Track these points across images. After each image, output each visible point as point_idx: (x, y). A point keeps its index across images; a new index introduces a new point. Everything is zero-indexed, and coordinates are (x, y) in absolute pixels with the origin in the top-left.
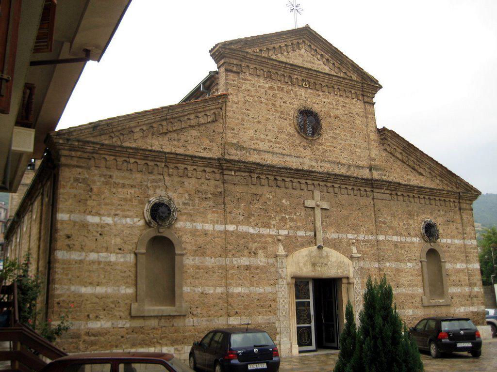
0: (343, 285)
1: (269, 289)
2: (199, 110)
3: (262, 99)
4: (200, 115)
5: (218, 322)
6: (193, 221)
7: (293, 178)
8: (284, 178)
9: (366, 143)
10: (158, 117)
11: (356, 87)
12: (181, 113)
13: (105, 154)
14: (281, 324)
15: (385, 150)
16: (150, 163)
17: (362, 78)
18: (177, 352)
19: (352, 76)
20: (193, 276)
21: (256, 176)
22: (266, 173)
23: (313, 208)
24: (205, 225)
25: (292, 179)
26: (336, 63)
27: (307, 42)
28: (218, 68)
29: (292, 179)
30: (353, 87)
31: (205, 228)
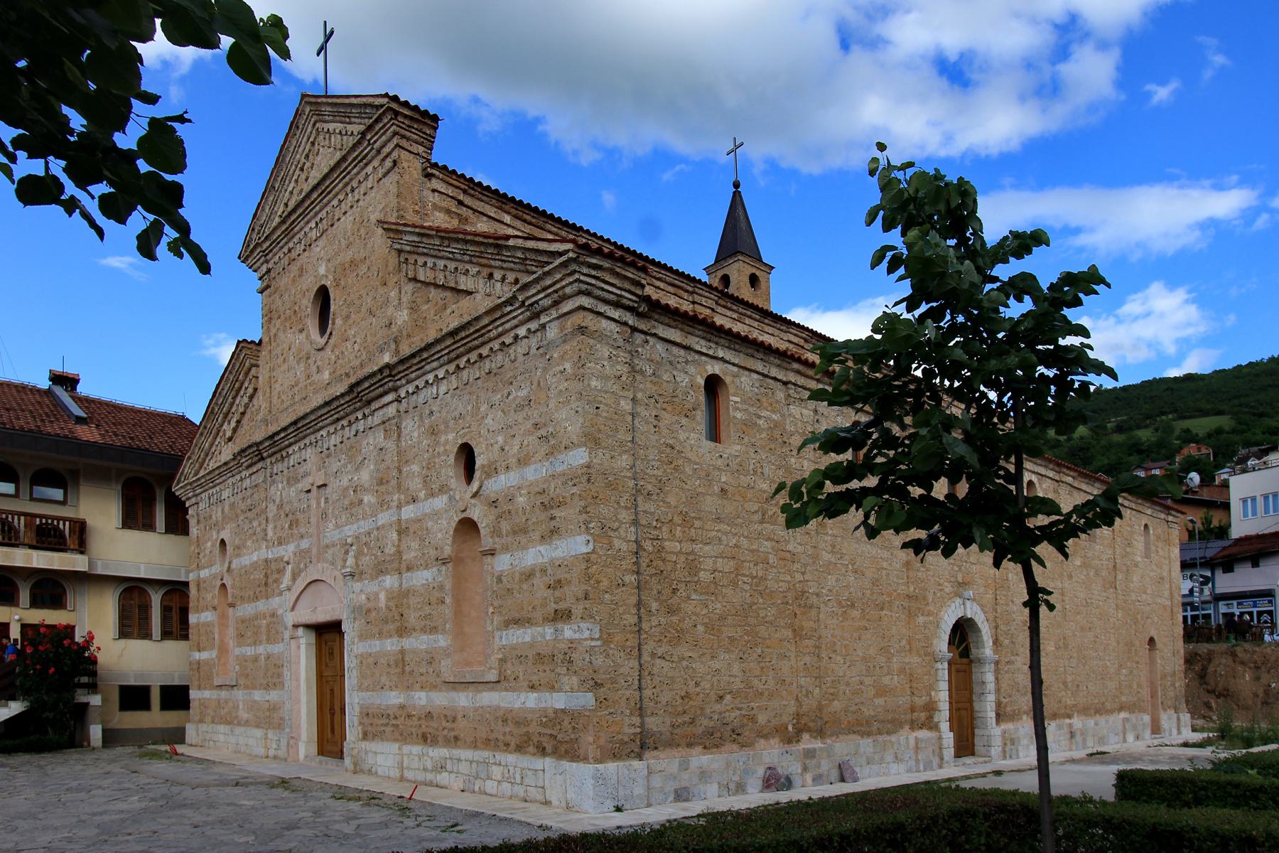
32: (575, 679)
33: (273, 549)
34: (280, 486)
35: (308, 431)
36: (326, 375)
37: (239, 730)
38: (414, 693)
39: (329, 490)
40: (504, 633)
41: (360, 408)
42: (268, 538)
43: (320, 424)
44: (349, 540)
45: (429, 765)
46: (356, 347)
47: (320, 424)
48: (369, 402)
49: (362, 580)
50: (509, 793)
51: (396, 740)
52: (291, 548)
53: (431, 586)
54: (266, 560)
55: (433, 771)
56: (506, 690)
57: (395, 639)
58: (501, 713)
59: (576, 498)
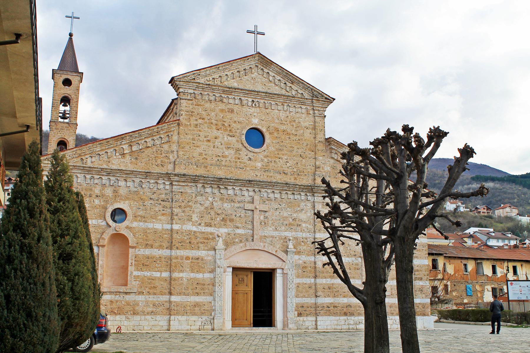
0: (278, 275)
1: (207, 275)
2: (154, 134)
3: (213, 121)
4: (155, 138)
5: (162, 299)
6: (145, 222)
7: (235, 186)
8: (226, 186)
9: (313, 153)
10: (119, 142)
11: (306, 103)
12: (138, 138)
13: (77, 173)
14: (217, 303)
15: (332, 158)
16: (112, 178)
17: (313, 94)
18: (127, 320)
19: (304, 93)
20: (143, 264)
21: (200, 185)
22: (210, 182)
23: (253, 210)
24: (155, 224)
25: (234, 187)
26: (287, 83)
27: (259, 66)
28: (178, 95)
29: (234, 187)
30: (303, 104)
31: (155, 227)
32: (424, 295)
33: (199, 227)
34: (210, 199)
35: (256, 186)
36: (259, 165)
37: (137, 318)
38: (339, 299)
39: (267, 214)
40: (391, 281)
41: (306, 192)
42: (193, 220)
43: (270, 187)
44: (291, 238)
45: (352, 322)
46: (288, 164)
47: (270, 187)
48: (314, 192)
49: (300, 255)
50: (396, 328)
51: (329, 315)
52: (223, 231)
53: (351, 263)
54: (191, 231)
55: (354, 324)
56: (392, 298)
57: (329, 280)
58: (390, 305)
59: (424, 251)
